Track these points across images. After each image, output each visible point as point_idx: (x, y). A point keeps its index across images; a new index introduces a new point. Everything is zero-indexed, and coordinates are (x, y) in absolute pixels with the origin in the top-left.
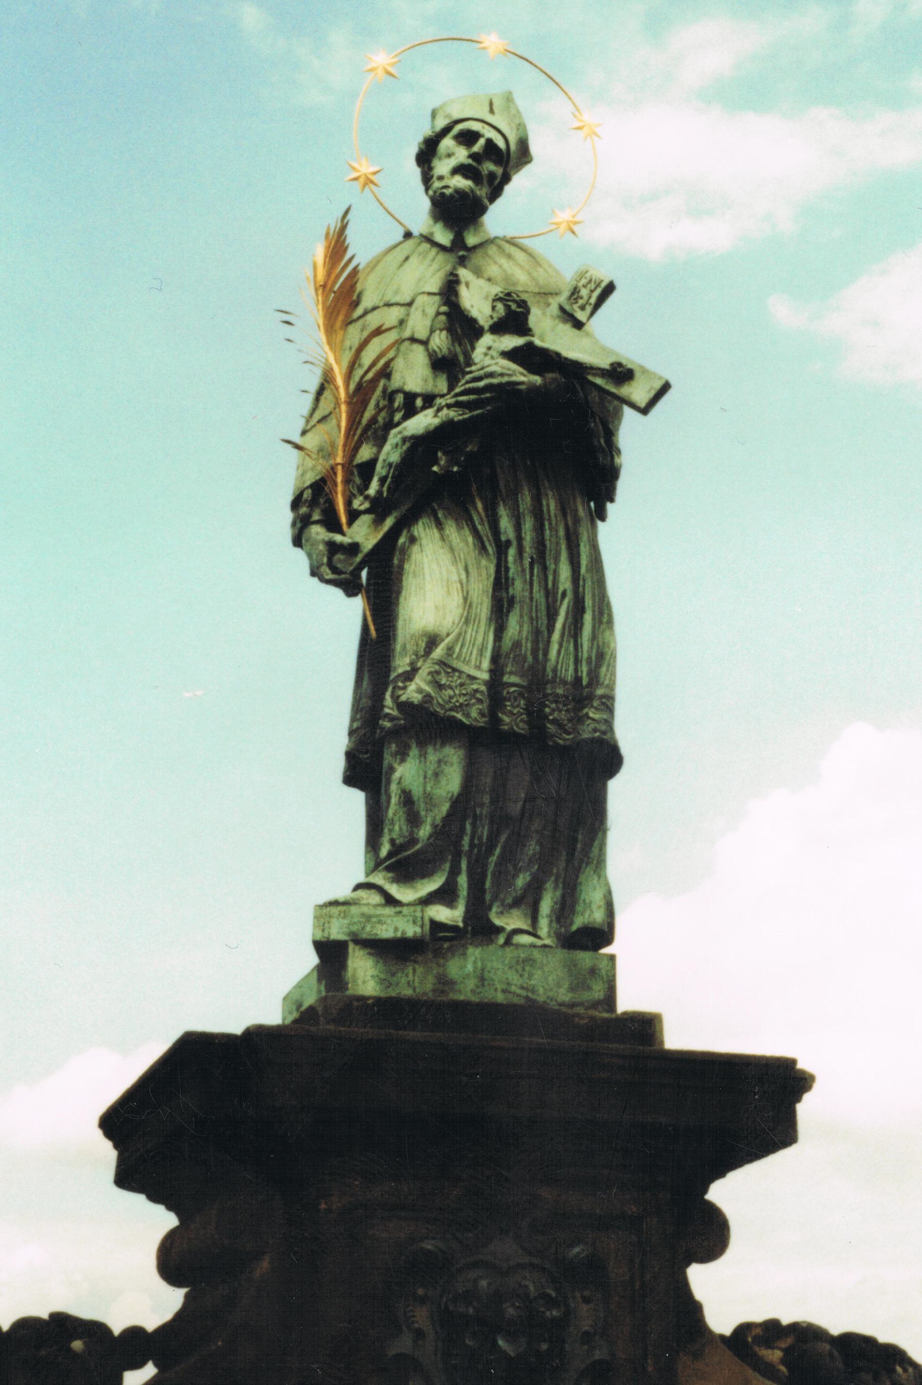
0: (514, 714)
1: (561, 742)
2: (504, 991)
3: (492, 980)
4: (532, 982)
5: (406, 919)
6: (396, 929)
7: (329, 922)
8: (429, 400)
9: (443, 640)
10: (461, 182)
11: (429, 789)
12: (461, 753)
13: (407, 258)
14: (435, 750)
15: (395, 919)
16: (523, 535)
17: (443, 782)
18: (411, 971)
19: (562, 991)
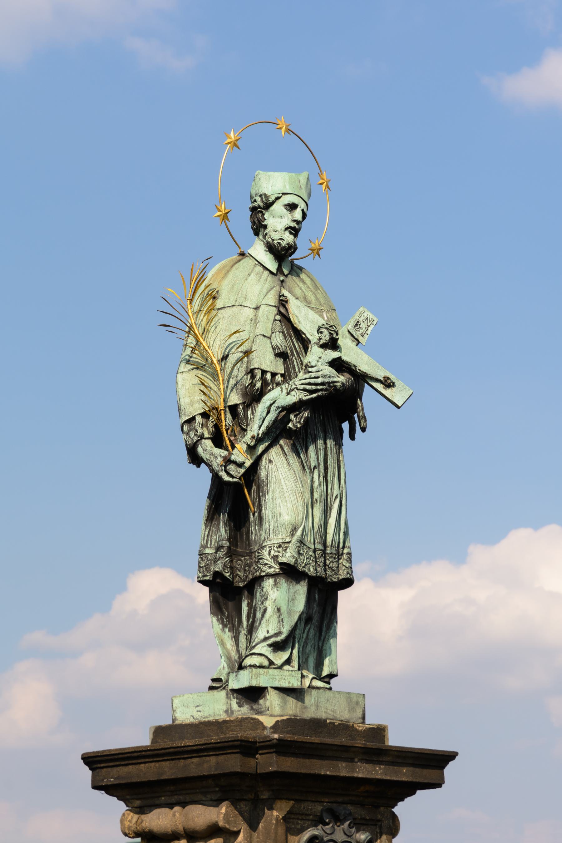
0: (321, 566)
1: (333, 579)
2: (326, 712)
3: (321, 707)
4: (335, 708)
5: (293, 678)
6: (289, 683)
7: (259, 677)
8: (274, 375)
9: (299, 528)
10: (289, 238)
11: (289, 607)
12: (305, 589)
13: (249, 275)
14: (293, 586)
15: (289, 677)
16: (320, 461)
17: (296, 604)
18: (291, 702)
19: (346, 712)
